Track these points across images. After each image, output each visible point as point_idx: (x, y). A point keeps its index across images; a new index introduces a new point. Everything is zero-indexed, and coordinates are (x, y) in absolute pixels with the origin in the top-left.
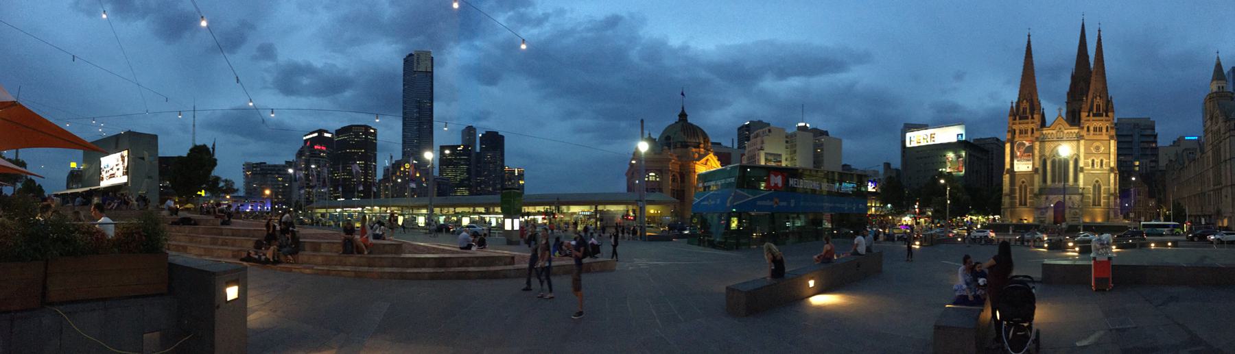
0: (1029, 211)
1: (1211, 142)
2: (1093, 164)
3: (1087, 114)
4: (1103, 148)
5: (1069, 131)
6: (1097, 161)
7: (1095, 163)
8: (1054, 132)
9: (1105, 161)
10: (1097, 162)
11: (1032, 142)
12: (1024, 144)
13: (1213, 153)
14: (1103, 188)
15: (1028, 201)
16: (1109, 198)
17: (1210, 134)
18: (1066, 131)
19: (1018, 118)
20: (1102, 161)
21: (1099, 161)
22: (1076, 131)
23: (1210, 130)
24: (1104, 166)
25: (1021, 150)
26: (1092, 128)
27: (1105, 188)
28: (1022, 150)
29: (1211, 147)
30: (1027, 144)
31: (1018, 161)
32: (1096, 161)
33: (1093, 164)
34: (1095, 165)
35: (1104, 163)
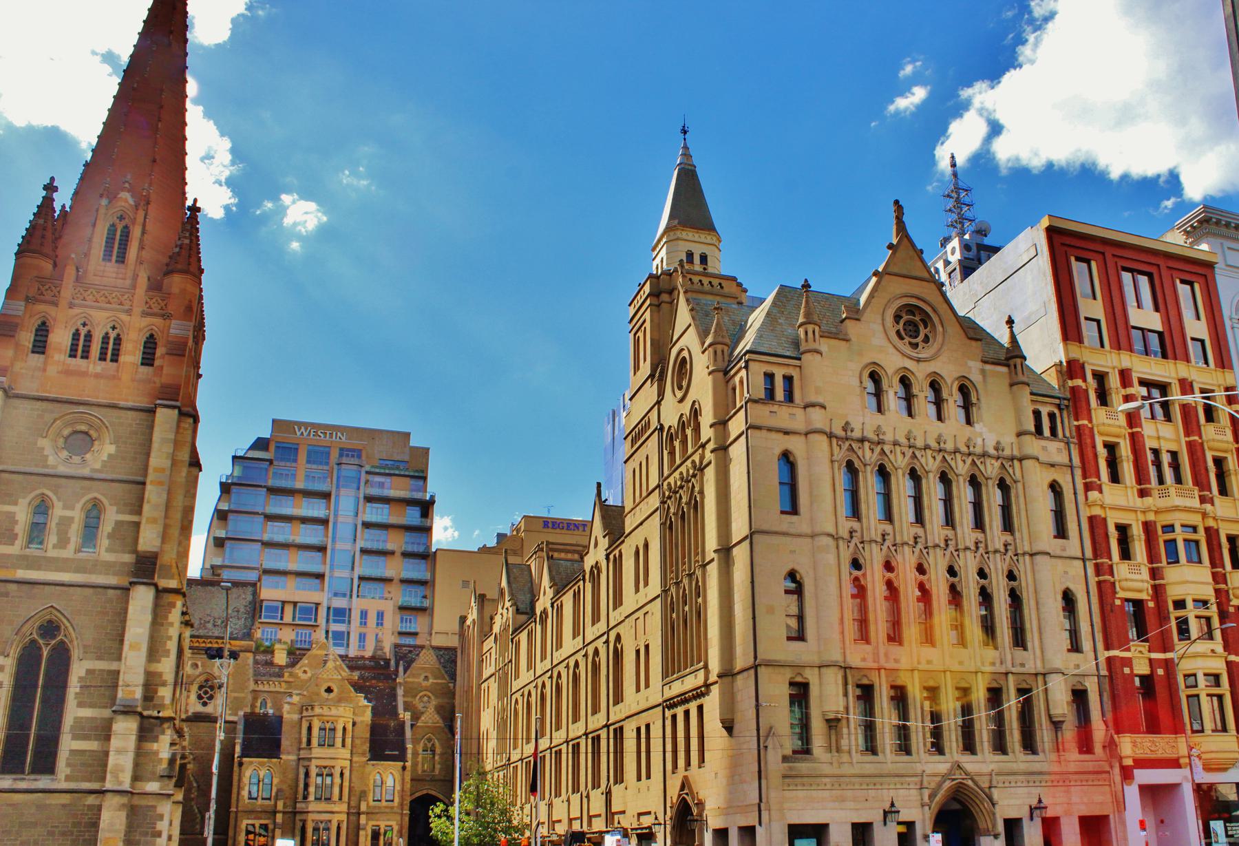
1: (654, 482)
2: (37, 531)
4: (110, 449)
7: (53, 525)
9: (112, 517)
13: (667, 526)
14: (78, 670)
16: (104, 732)
17: (653, 442)
20: (94, 514)
21: (77, 514)
23: (654, 424)
26: (60, 338)
27: (89, 672)
29: (654, 501)
32: (58, 511)
33: (37, 531)
34: (52, 539)
35: (107, 527)
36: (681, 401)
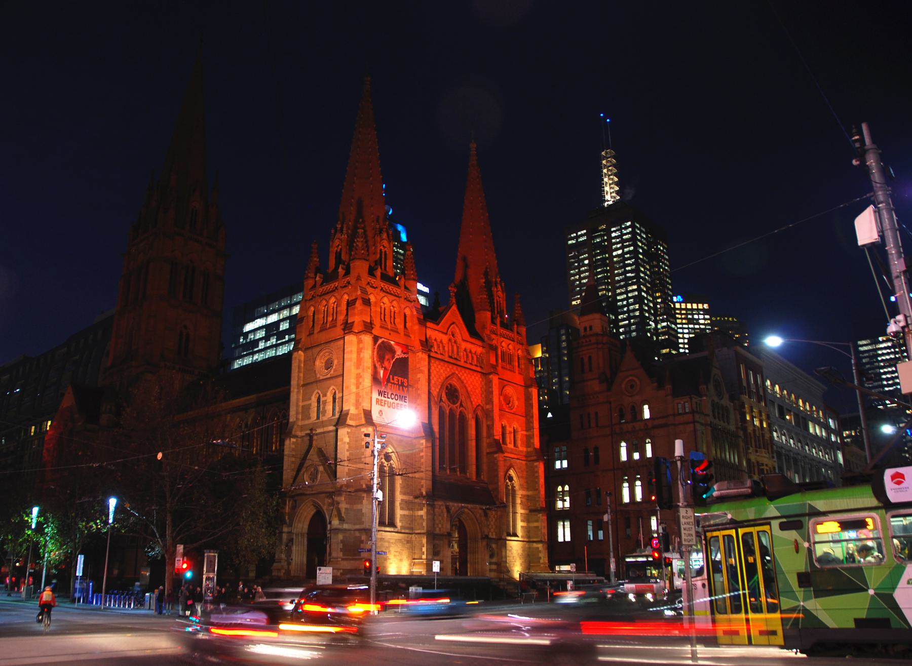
0: (400, 540)
3: (489, 314)
5: (469, 346)
6: (509, 429)
8: (445, 339)
10: (510, 433)
11: (406, 348)
12: (393, 352)
15: (399, 513)
18: (464, 345)
19: (378, 273)
21: (512, 430)
22: (479, 350)
24: (519, 443)
25: (386, 363)
28: (389, 365)
30: (399, 353)
31: (380, 393)
36: (631, 396)
